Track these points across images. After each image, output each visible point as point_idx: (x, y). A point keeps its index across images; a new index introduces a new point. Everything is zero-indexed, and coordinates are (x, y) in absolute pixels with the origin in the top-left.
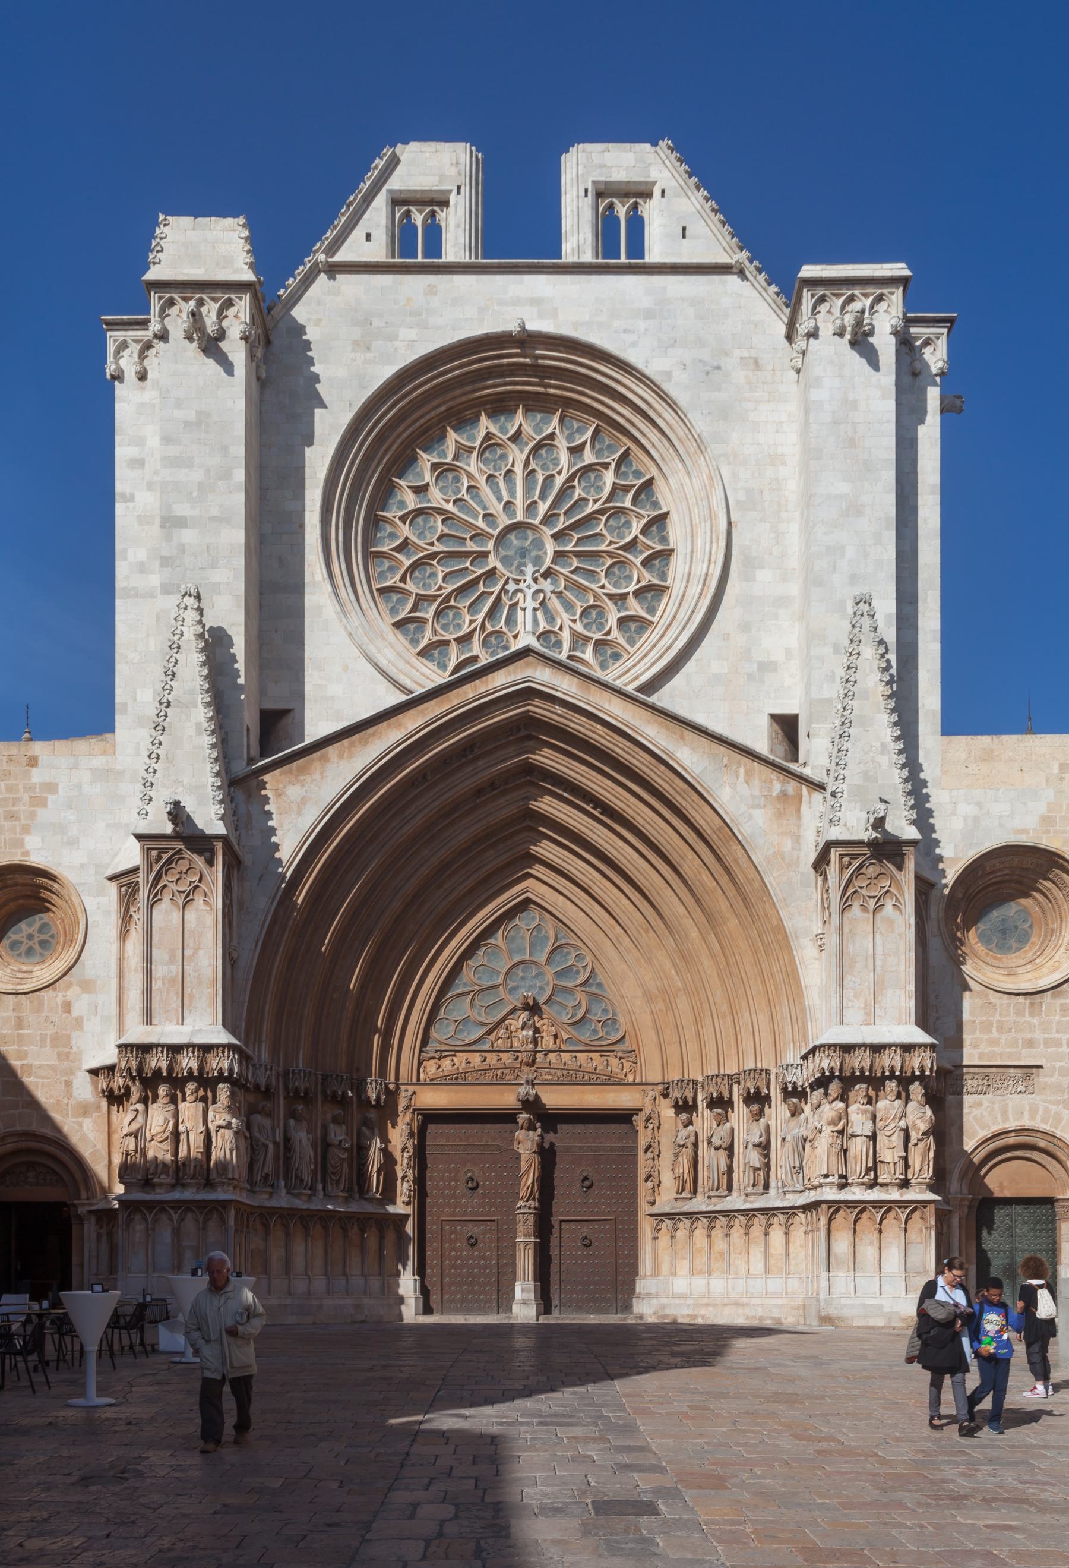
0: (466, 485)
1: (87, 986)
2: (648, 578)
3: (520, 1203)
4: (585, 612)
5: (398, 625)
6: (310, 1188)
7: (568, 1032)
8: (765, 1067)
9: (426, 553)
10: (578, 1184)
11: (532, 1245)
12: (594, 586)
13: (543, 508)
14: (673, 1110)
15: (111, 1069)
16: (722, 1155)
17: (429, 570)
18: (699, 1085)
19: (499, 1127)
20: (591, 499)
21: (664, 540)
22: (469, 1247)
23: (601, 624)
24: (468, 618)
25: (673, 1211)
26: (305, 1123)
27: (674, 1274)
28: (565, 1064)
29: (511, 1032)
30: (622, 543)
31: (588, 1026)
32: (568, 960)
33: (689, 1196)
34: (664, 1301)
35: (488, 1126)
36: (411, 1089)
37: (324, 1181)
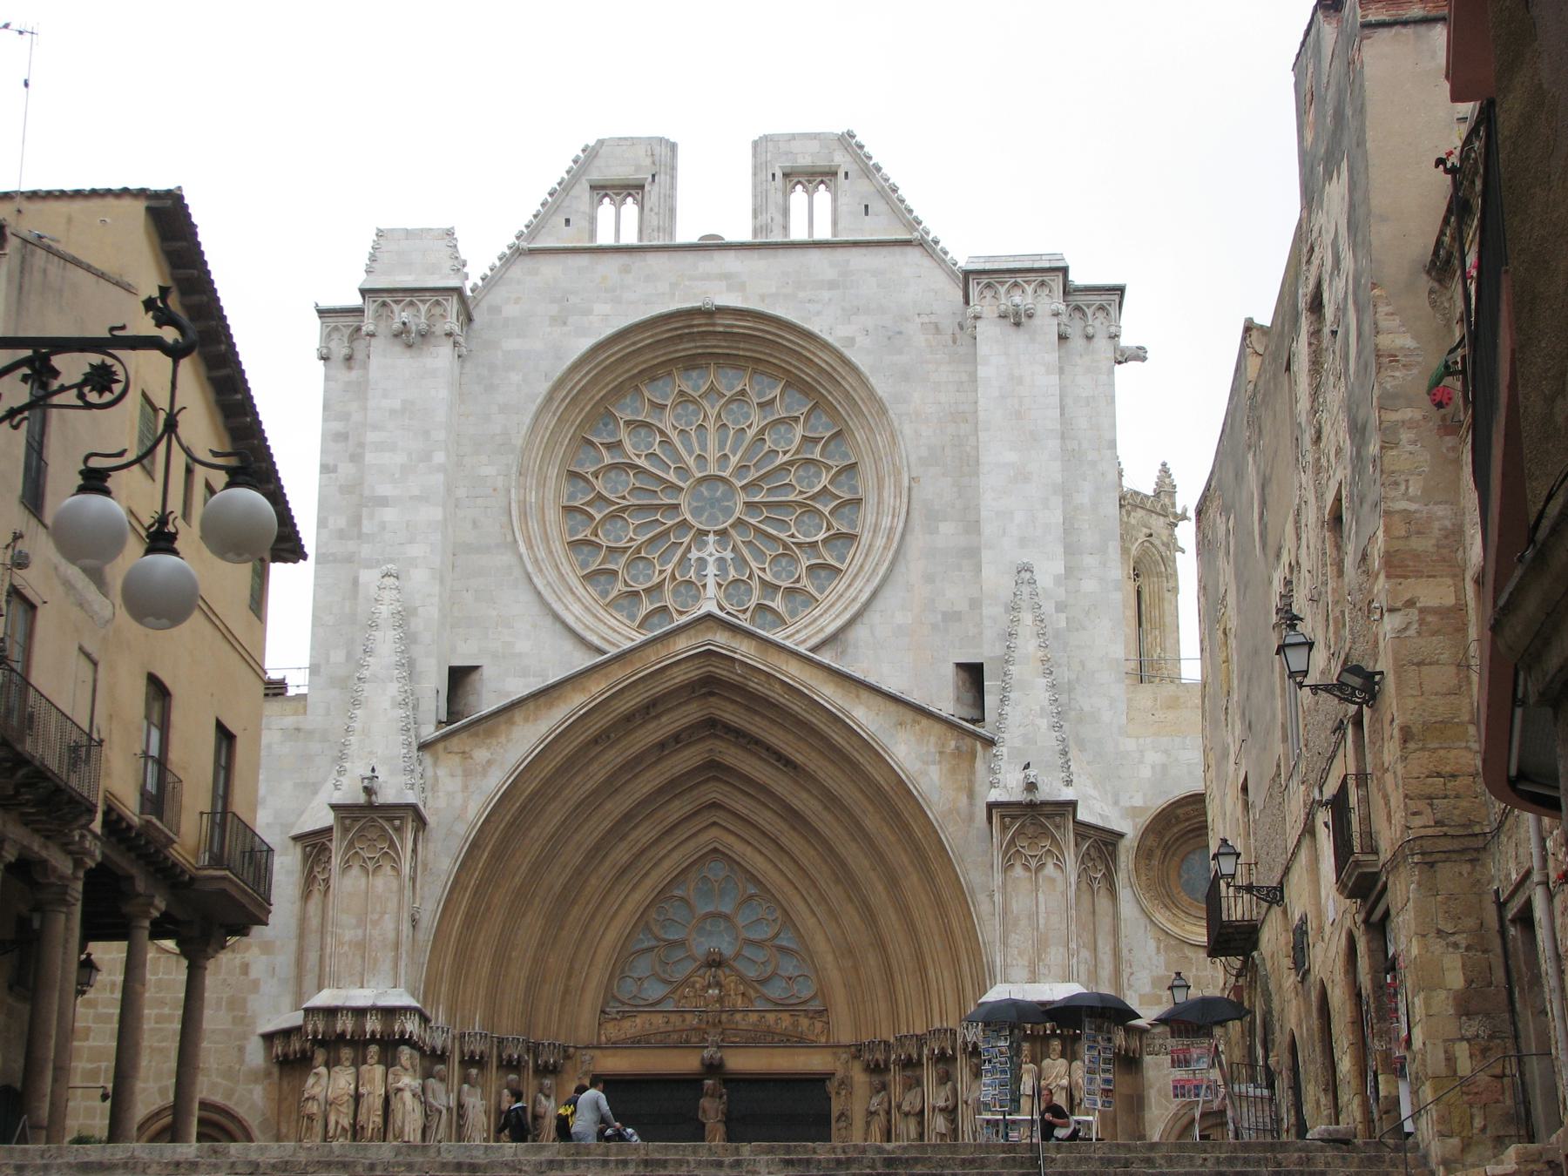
0: (658, 439)
1: (267, 948)
2: (840, 526)
4: (775, 559)
5: (589, 578)
7: (757, 991)
8: (951, 1025)
9: (617, 507)
12: (783, 536)
13: (734, 460)
15: (286, 1034)
17: (620, 523)
20: (780, 450)
21: (854, 489)
23: (791, 572)
24: (658, 568)
30: (811, 494)
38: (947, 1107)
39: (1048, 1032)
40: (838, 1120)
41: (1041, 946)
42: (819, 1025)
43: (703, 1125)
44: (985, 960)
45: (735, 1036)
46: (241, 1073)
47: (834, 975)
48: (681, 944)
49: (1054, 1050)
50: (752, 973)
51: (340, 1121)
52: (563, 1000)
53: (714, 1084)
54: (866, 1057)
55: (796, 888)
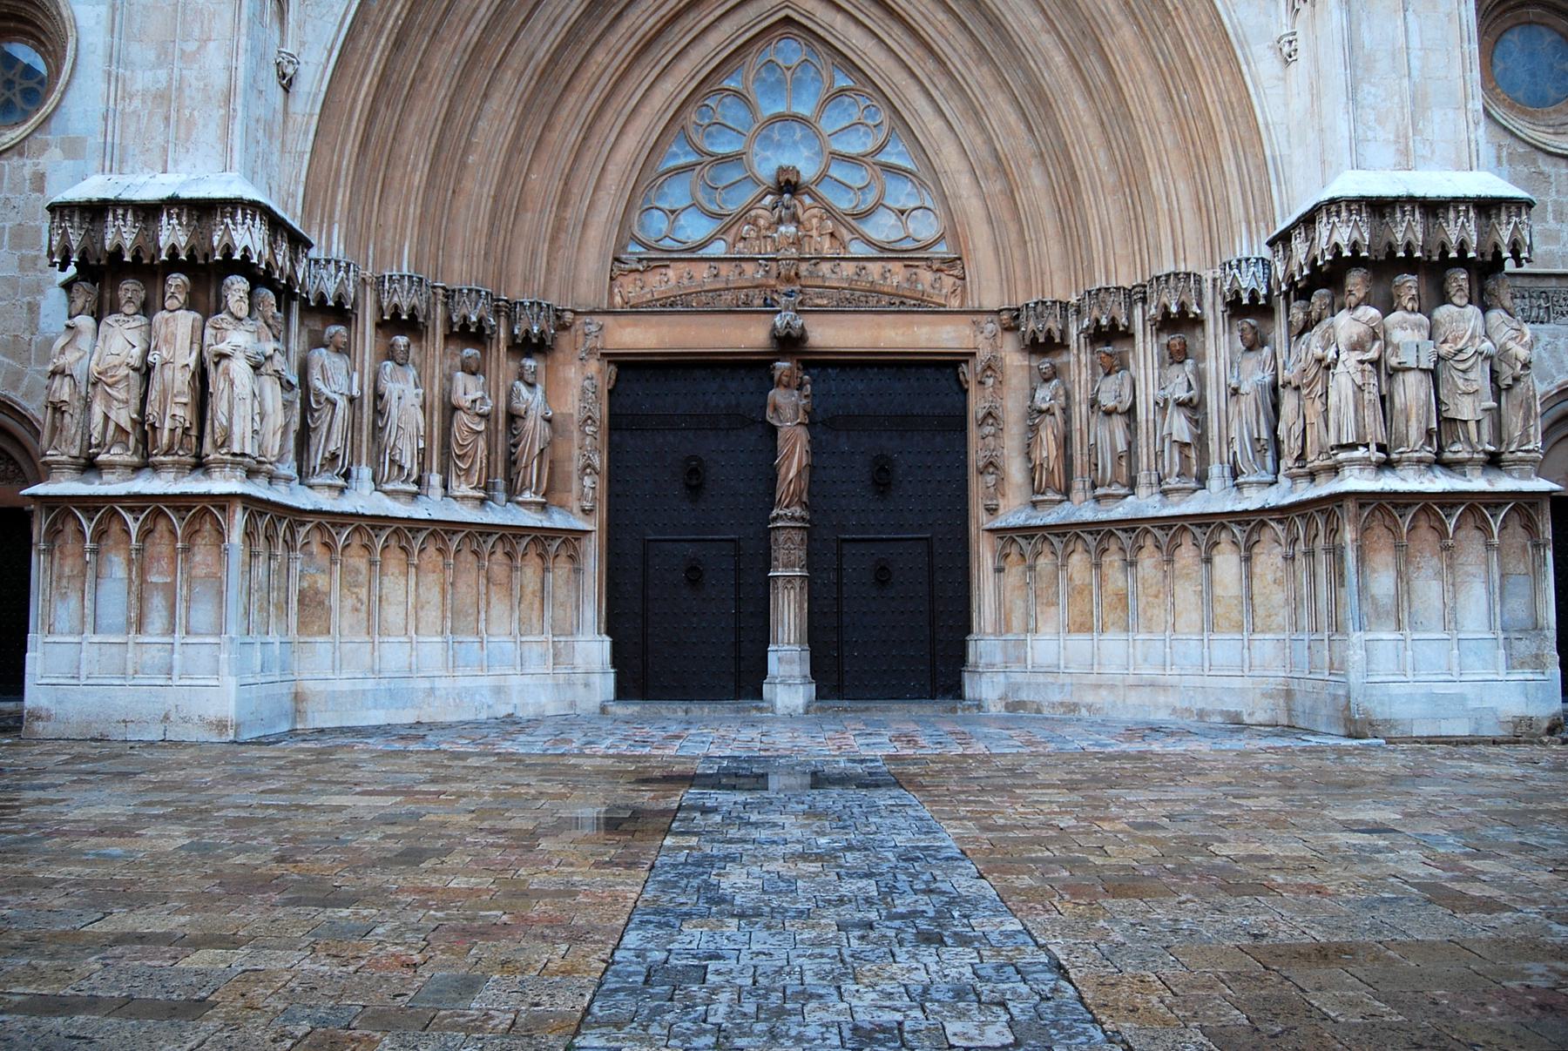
6: (419, 482)
7: (852, 230)
16: (1118, 423)
18: (1071, 310)
26: (412, 373)
37: (445, 471)
38: (1191, 400)
39: (1453, 254)
41: (1418, 104)
42: (948, 281)
43: (774, 430)
44: (1268, 153)
45: (821, 296)
46: (33, 348)
47: (970, 204)
48: (735, 159)
49: (1460, 288)
50: (844, 203)
51: (113, 415)
52: (554, 239)
53: (790, 368)
54: (1032, 325)
55: (913, 75)
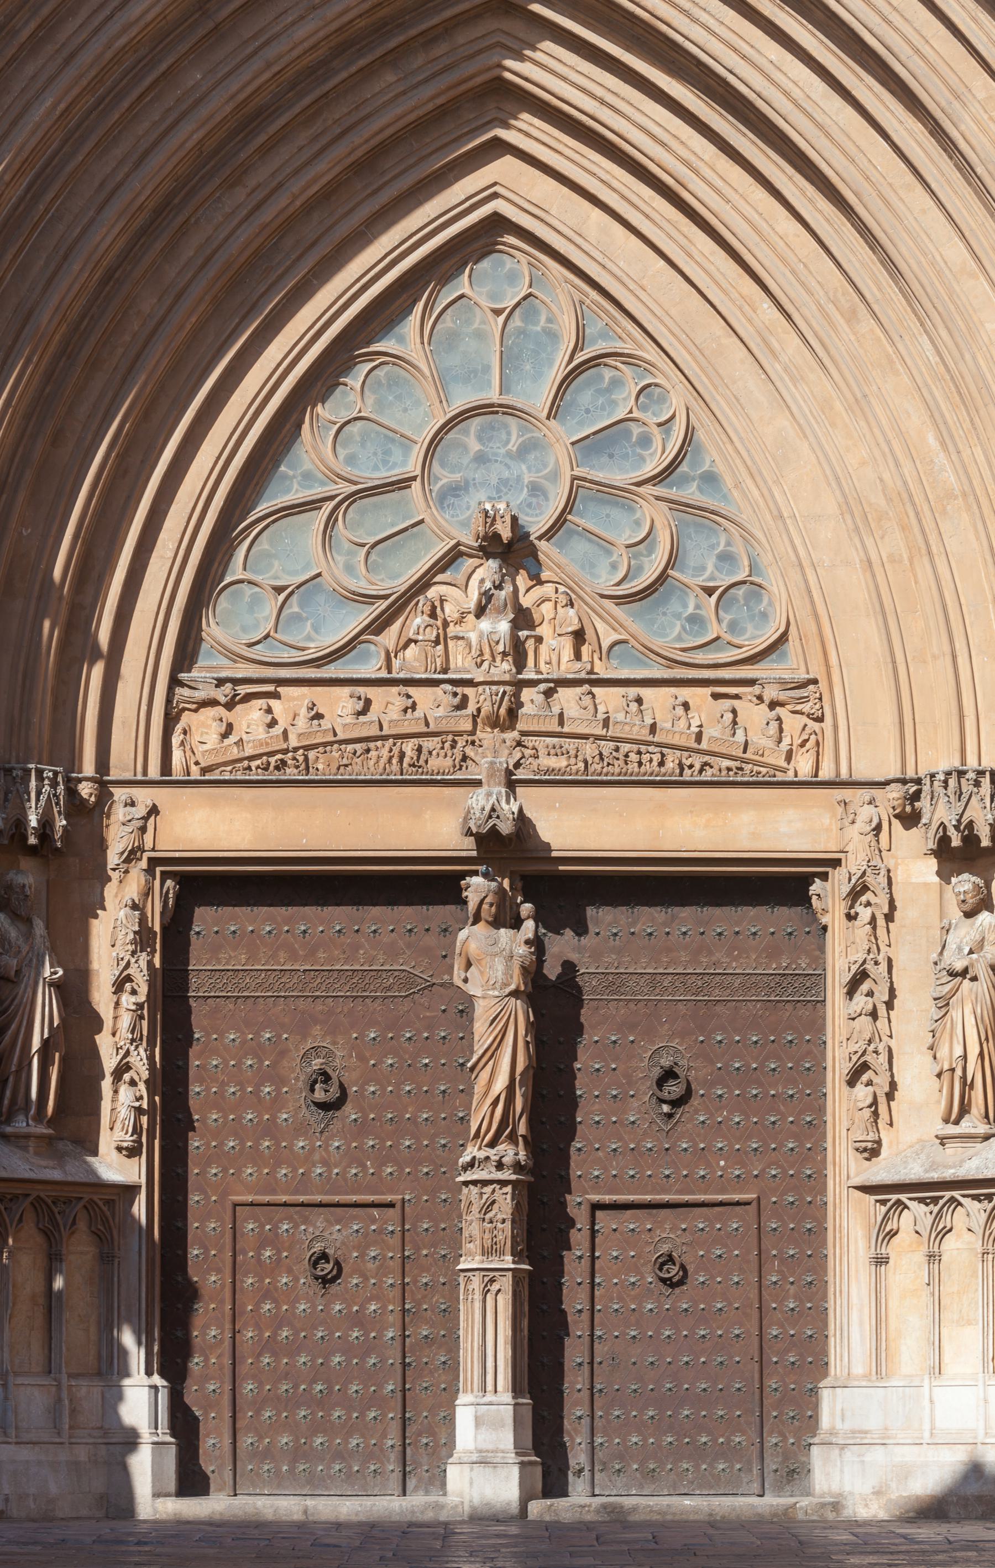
3: (472, 1151)
10: (646, 1090)
11: (506, 1283)
14: (933, 863)
19: (407, 914)
22: (317, 1287)
25: (935, 1176)
27: (938, 1370)
28: (606, 723)
29: (446, 624)
31: (674, 606)
32: (614, 403)
33: (983, 1129)
34: (906, 1454)
35: (376, 911)
36: (145, 797)
40: (852, 988)
42: (793, 724)
